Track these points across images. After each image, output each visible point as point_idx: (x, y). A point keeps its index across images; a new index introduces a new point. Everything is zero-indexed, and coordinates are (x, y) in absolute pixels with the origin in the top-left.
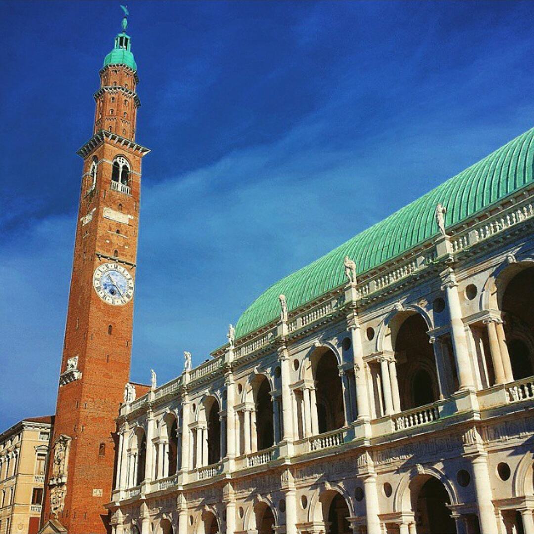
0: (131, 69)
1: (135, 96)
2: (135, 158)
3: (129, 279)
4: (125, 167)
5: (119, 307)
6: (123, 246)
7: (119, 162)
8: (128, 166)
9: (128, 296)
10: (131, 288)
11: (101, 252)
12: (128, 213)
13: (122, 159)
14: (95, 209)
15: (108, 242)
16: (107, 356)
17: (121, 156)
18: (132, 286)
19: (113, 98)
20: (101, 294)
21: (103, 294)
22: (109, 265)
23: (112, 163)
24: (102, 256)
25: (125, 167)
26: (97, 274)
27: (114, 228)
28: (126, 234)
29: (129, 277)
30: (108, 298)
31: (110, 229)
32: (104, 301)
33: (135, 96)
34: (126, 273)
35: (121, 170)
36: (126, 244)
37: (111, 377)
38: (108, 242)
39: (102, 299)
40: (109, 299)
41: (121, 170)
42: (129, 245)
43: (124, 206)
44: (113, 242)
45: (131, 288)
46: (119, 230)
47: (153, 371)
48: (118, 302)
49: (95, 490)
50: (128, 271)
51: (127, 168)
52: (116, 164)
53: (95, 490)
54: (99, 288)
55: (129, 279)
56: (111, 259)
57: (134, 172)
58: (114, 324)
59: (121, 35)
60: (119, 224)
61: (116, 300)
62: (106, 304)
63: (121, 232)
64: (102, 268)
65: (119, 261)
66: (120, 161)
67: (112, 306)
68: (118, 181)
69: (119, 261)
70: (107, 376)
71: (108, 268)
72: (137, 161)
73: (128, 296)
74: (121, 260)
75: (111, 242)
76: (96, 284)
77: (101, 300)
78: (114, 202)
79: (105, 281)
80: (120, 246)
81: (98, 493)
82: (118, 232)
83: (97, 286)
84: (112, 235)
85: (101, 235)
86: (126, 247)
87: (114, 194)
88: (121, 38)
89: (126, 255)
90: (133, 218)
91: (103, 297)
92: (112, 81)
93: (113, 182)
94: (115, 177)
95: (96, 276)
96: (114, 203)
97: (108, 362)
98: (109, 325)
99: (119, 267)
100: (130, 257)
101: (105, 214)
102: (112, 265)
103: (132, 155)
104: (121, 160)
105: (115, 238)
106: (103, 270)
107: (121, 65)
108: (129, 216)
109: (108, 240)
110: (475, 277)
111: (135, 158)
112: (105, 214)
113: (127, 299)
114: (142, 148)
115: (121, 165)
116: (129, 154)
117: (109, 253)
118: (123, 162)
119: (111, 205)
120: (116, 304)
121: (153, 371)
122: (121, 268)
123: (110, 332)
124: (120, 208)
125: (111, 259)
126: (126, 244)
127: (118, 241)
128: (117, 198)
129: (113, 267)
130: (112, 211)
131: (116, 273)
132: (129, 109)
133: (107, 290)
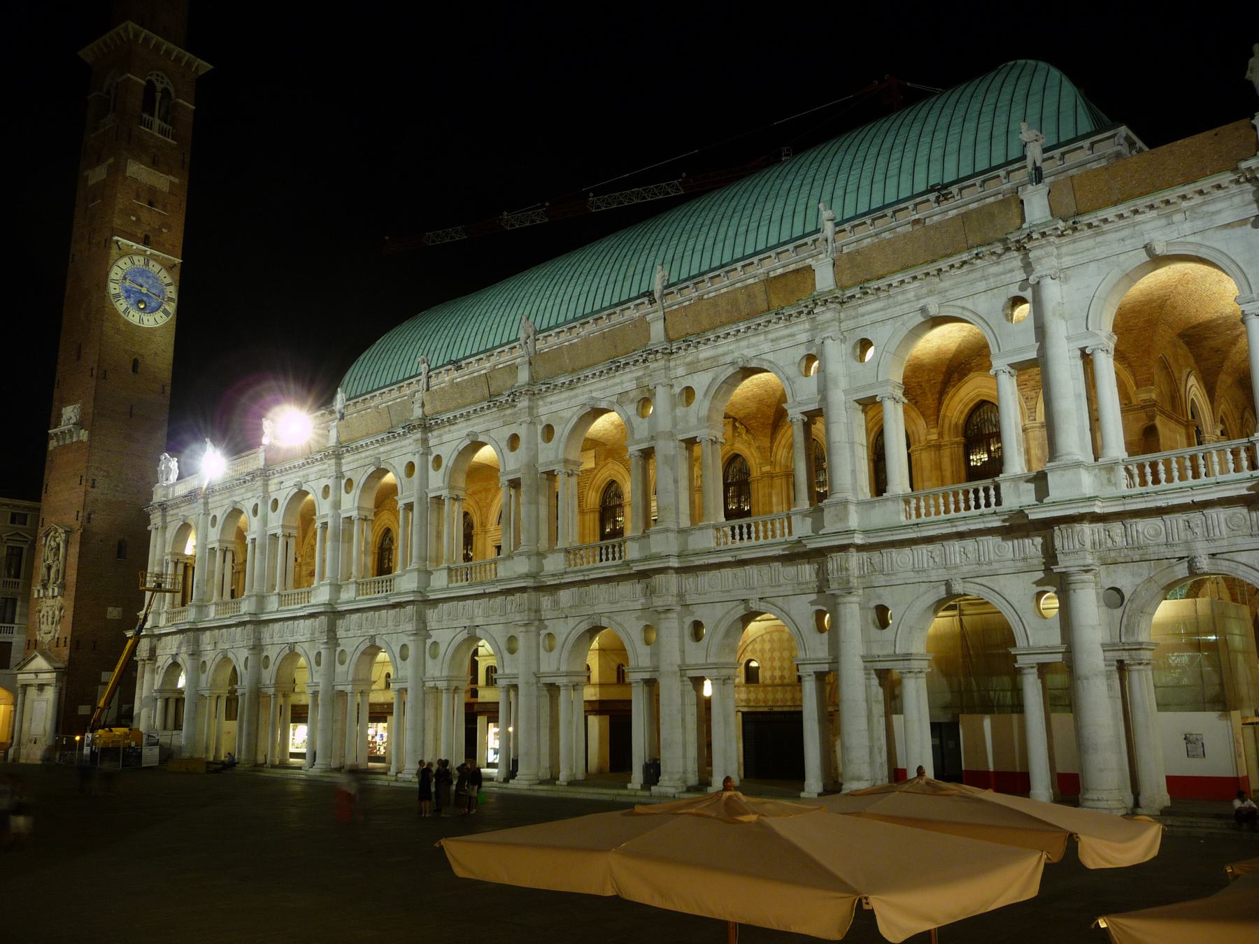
4: (166, 92)
5: (151, 331)
8: (172, 89)
9: (166, 312)
10: (170, 299)
12: (169, 173)
14: (111, 160)
20: (121, 305)
21: (124, 306)
25: (166, 92)
26: (116, 273)
28: (164, 208)
29: (168, 280)
30: (132, 313)
31: (138, 197)
35: (159, 95)
36: (163, 225)
40: (134, 317)
41: (159, 95)
42: (169, 229)
49: (110, 609)
52: (150, 83)
53: (110, 609)
54: (117, 296)
57: (181, 101)
60: (152, 190)
62: (128, 324)
68: (152, 115)
71: (133, 263)
75: (138, 219)
76: (114, 288)
77: (119, 316)
81: (113, 613)
82: (151, 204)
83: (113, 292)
84: (142, 207)
90: (177, 181)
91: (125, 312)
93: (145, 116)
94: (148, 106)
95: (113, 276)
99: (151, 263)
106: (124, 267)
108: (172, 178)
110: (695, 376)
115: (159, 86)
124: (154, 164)
126: (163, 225)
129: (142, 262)
133: (132, 301)
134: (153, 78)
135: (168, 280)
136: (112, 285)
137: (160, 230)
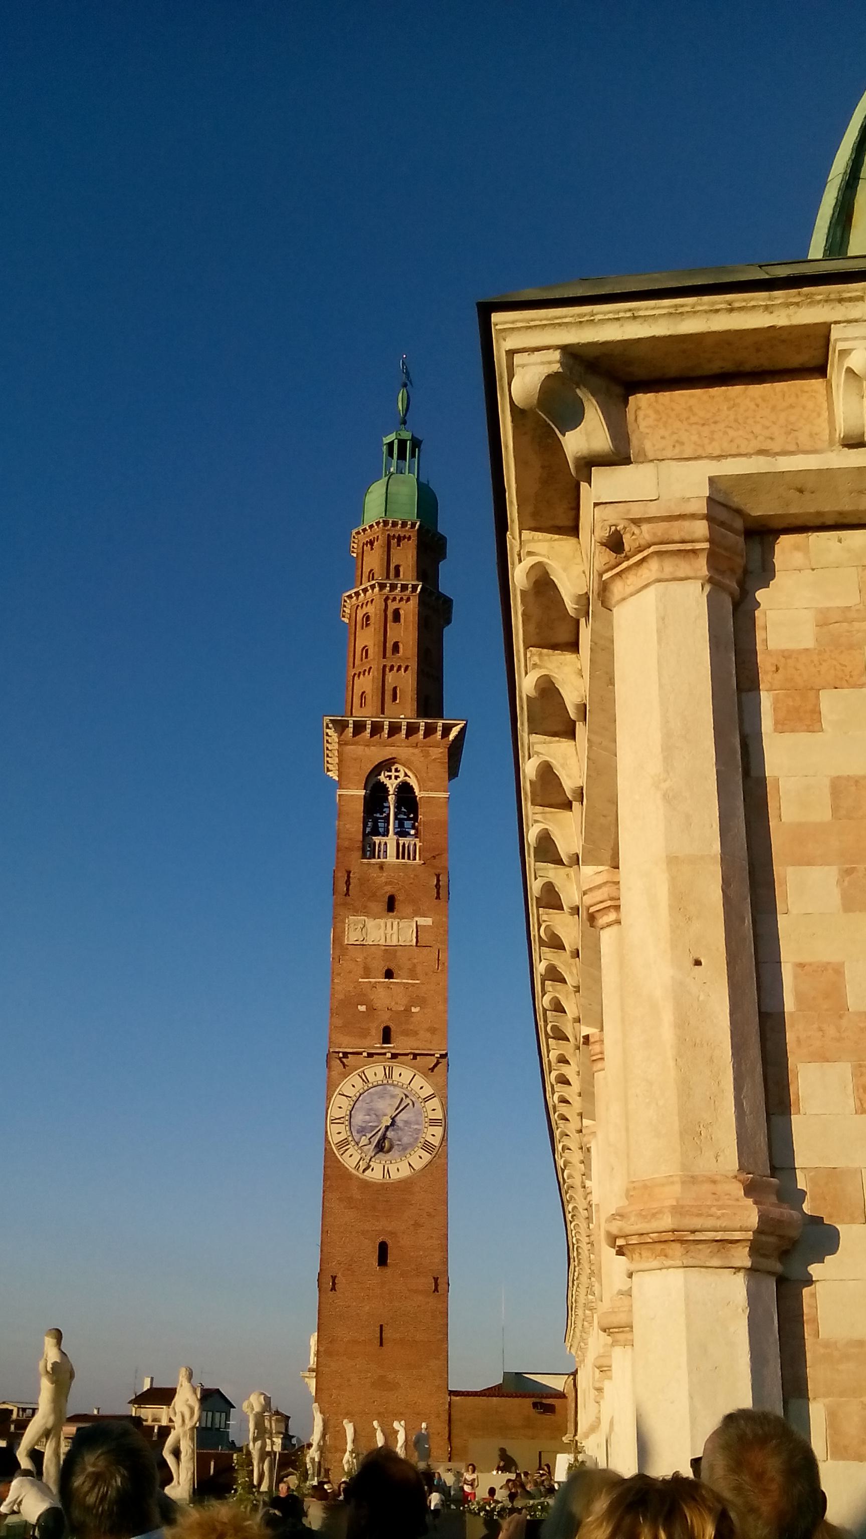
0: (404, 524)
1: (419, 590)
2: (426, 755)
3: (426, 1099)
5: (405, 1185)
6: (407, 1010)
7: (387, 782)
8: (413, 782)
9: (427, 1146)
10: (433, 1122)
11: (347, 1044)
13: (397, 770)
15: (362, 1008)
16: (378, 1329)
17: (387, 765)
18: (439, 1115)
19: (367, 617)
20: (350, 1160)
22: (369, 1073)
23: (363, 792)
24: (346, 1055)
25: (405, 789)
27: (380, 966)
28: (413, 974)
29: (428, 1090)
31: (367, 973)
32: (361, 1176)
33: (419, 590)
34: (419, 1081)
37: (393, 1387)
38: (362, 1008)
39: (354, 1172)
41: (391, 799)
43: (400, 897)
44: (378, 1004)
45: (433, 1122)
46: (392, 966)
47: (375, 1423)
48: (398, 1169)
50: (425, 1075)
51: (412, 788)
55: (426, 1099)
56: (370, 1055)
58: (392, 1234)
59: (387, 440)
60: (390, 952)
61: (392, 1168)
62: (366, 1185)
63: (395, 971)
64: (351, 1085)
65: (394, 1056)
66: (390, 777)
67: (382, 1185)
68: (386, 833)
69: (394, 1056)
70: (382, 1384)
71: (366, 1081)
72: (436, 759)
73: (427, 1146)
74: (393, 1051)
75: (371, 1009)
78: (374, 895)
79: (359, 1118)
80: (397, 1012)
82: (389, 974)
84: (374, 986)
85: (341, 997)
86: (413, 1010)
87: (374, 873)
88: (391, 445)
89: (416, 1033)
92: (366, 570)
95: (334, 1112)
96: (373, 896)
97: (381, 1345)
98: (380, 1239)
100: (428, 1035)
101: (352, 937)
102: (375, 1072)
103: (416, 751)
104: (393, 774)
105: (381, 992)
106: (351, 1092)
107: (378, 523)
109: (362, 1005)
111: (426, 755)
112: (352, 937)
113: (427, 1157)
114: (440, 724)
115: (392, 785)
116: (411, 750)
117: (369, 1038)
118: (397, 777)
119: (365, 907)
120: (395, 1176)
121: (375, 1423)
122: (403, 1074)
123: (383, 1260)
124: (391, 905)
125: (370, 1055)
127: (387, 997)
128: (383, 879)
130: (371, 923)
131: (392, 1088)
132: (406, 629)
134: (382, 778)
135: (428, 1090)
136: (333, 1129)
137: (407, 1010)
